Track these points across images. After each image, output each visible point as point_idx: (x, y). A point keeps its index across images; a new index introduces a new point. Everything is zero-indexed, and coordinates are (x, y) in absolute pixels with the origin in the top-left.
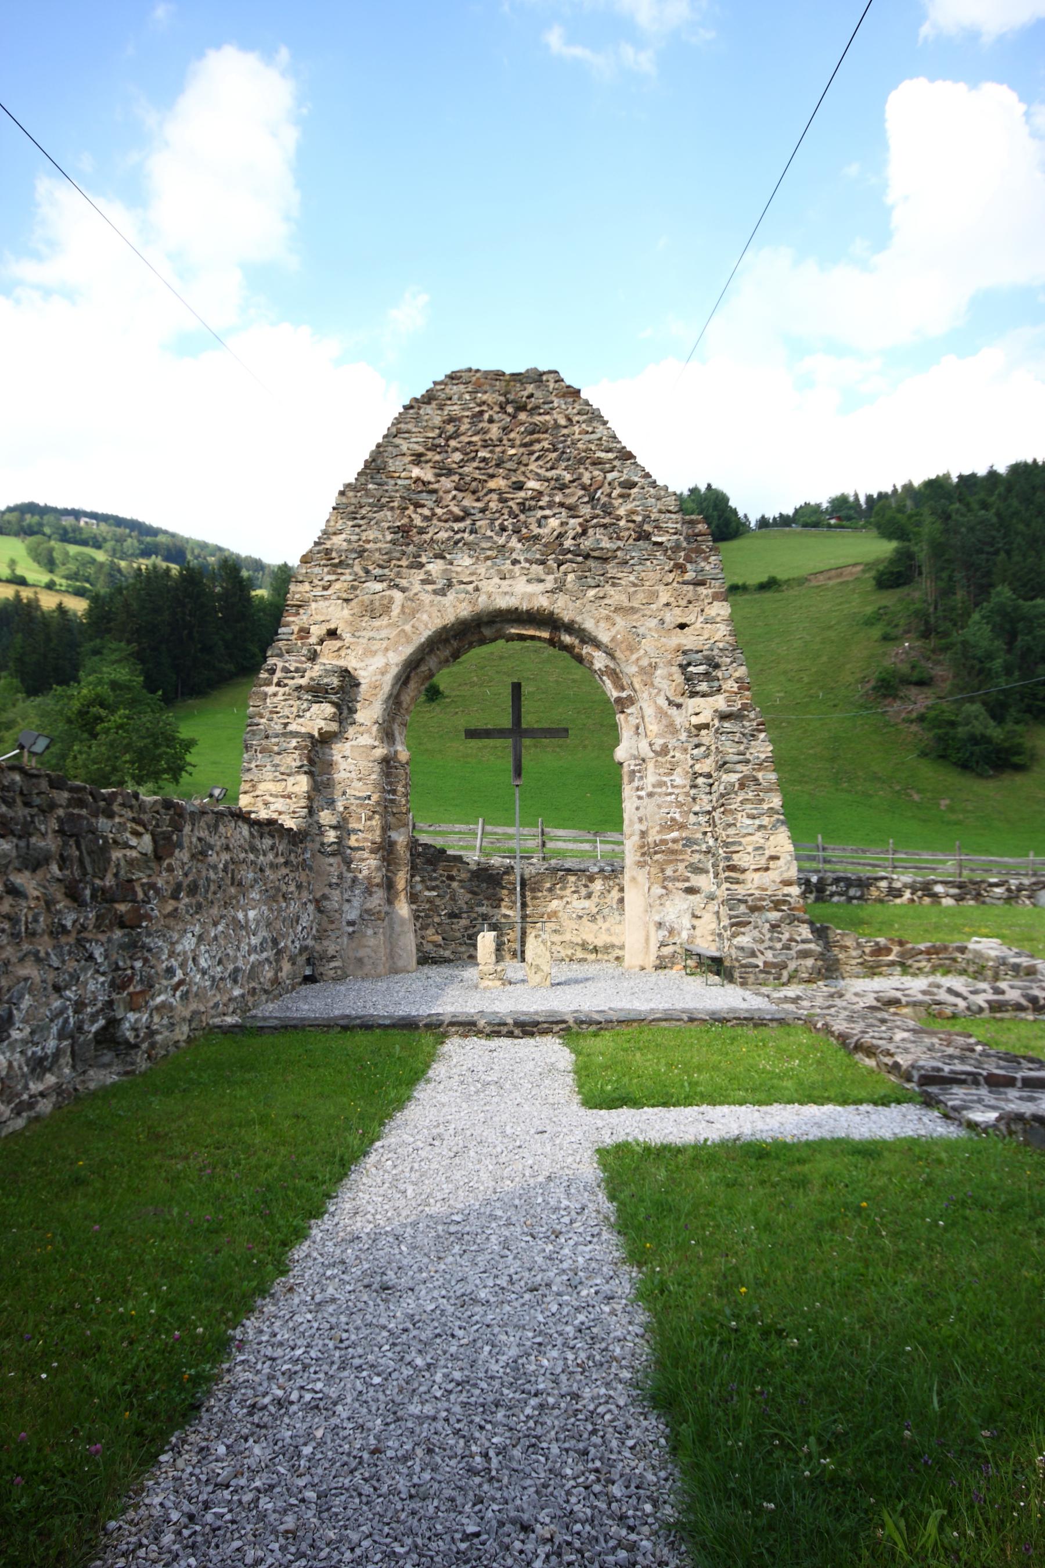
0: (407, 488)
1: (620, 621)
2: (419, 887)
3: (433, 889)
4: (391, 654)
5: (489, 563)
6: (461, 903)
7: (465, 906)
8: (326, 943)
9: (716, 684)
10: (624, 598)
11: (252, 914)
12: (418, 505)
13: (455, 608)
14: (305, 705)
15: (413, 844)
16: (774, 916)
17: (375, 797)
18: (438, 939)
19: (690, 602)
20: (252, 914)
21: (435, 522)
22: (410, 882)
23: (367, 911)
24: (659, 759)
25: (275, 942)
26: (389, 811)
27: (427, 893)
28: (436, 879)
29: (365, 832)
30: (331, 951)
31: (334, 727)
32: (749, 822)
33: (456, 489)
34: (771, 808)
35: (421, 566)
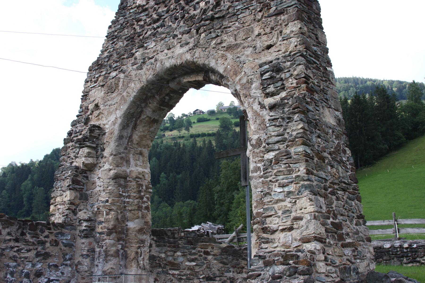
0: (136, 13)
1: (229, 56)
3: (193, 260)
4: (118, 112)
5: (163, 42)
6: (215, 270)
7: (217, 273)
9: (279, 84)
10: (232, 39)
12: (139, 20)
13: (147, 74)
14: (78, 150)
16: (279, 269)
17: (110, 200)
19: (272, 29)
21: (146, 27)
24: (256, 150)
27: (187, 263)
28: (195, 254)
32: (279, 190)
33: (156, 4)
34: (298, 176)
35: (133, 54)
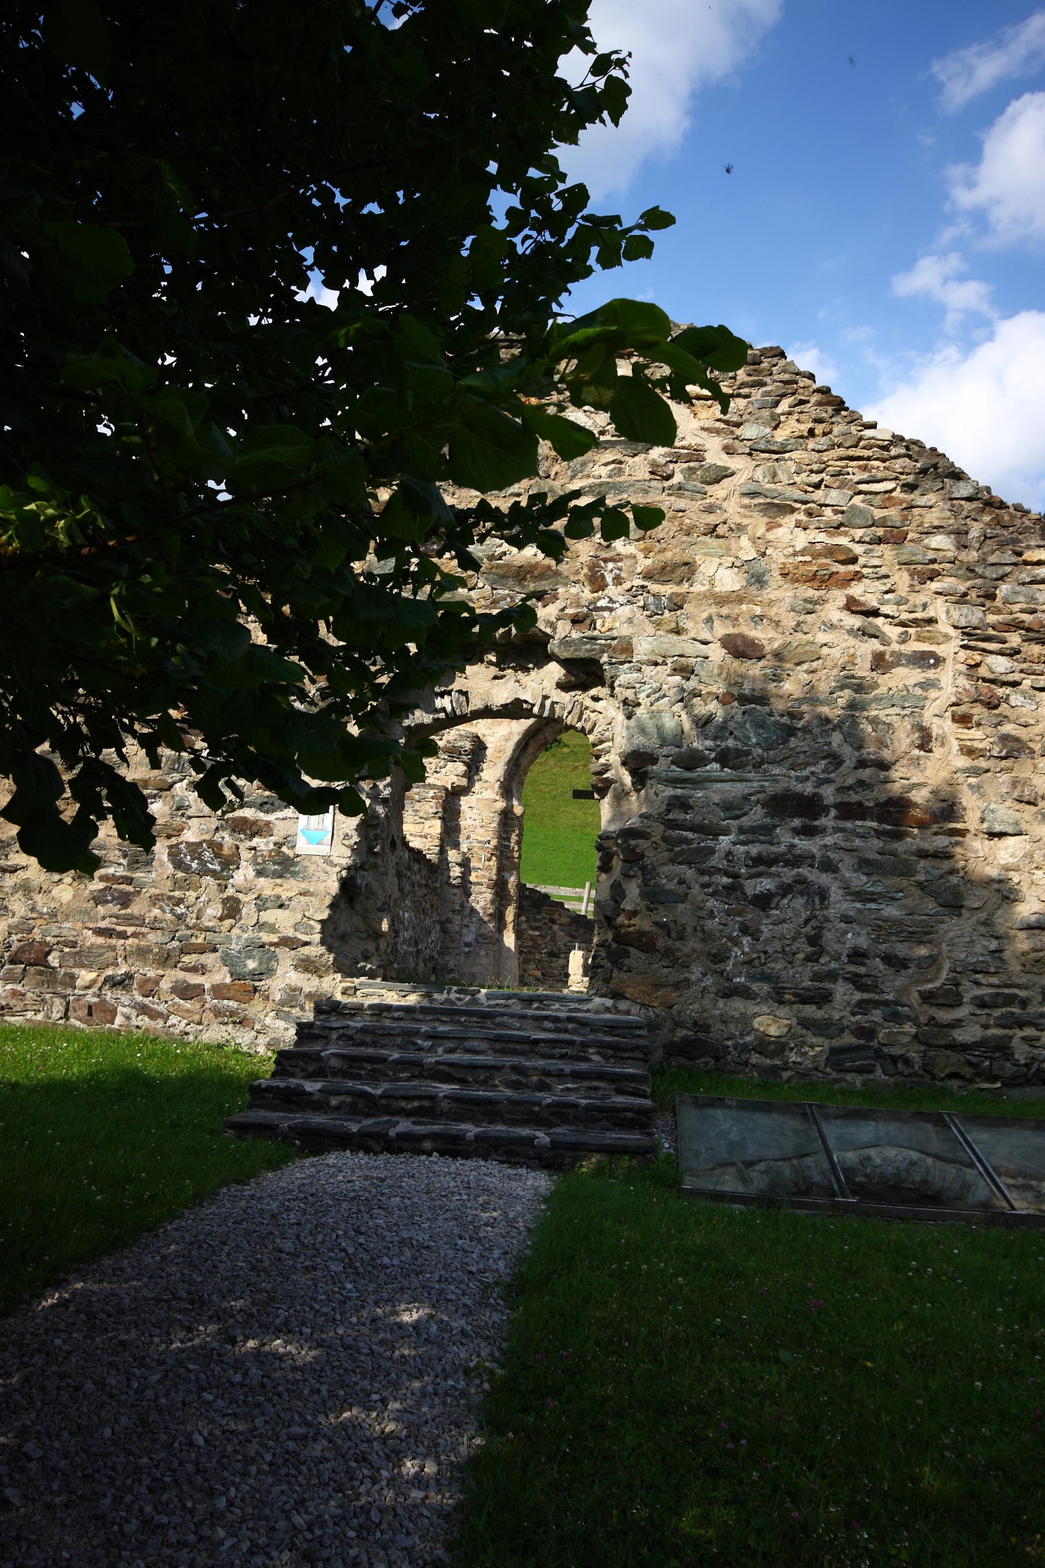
2: (524, 926)
8: (447, 958)
11: (407, 915)
14: (442, 763)
15: (521, 887)
17: (494, 842)
18: (539, 974)
20: (407, 915)
22: (517, 916)
23: (482, 935)
25: (416, 944)
26: (503, 854)
27: (531, 932)
28: (539, 920)
29: (483, 872)
30: (451, 965)
31: (464, 782)
